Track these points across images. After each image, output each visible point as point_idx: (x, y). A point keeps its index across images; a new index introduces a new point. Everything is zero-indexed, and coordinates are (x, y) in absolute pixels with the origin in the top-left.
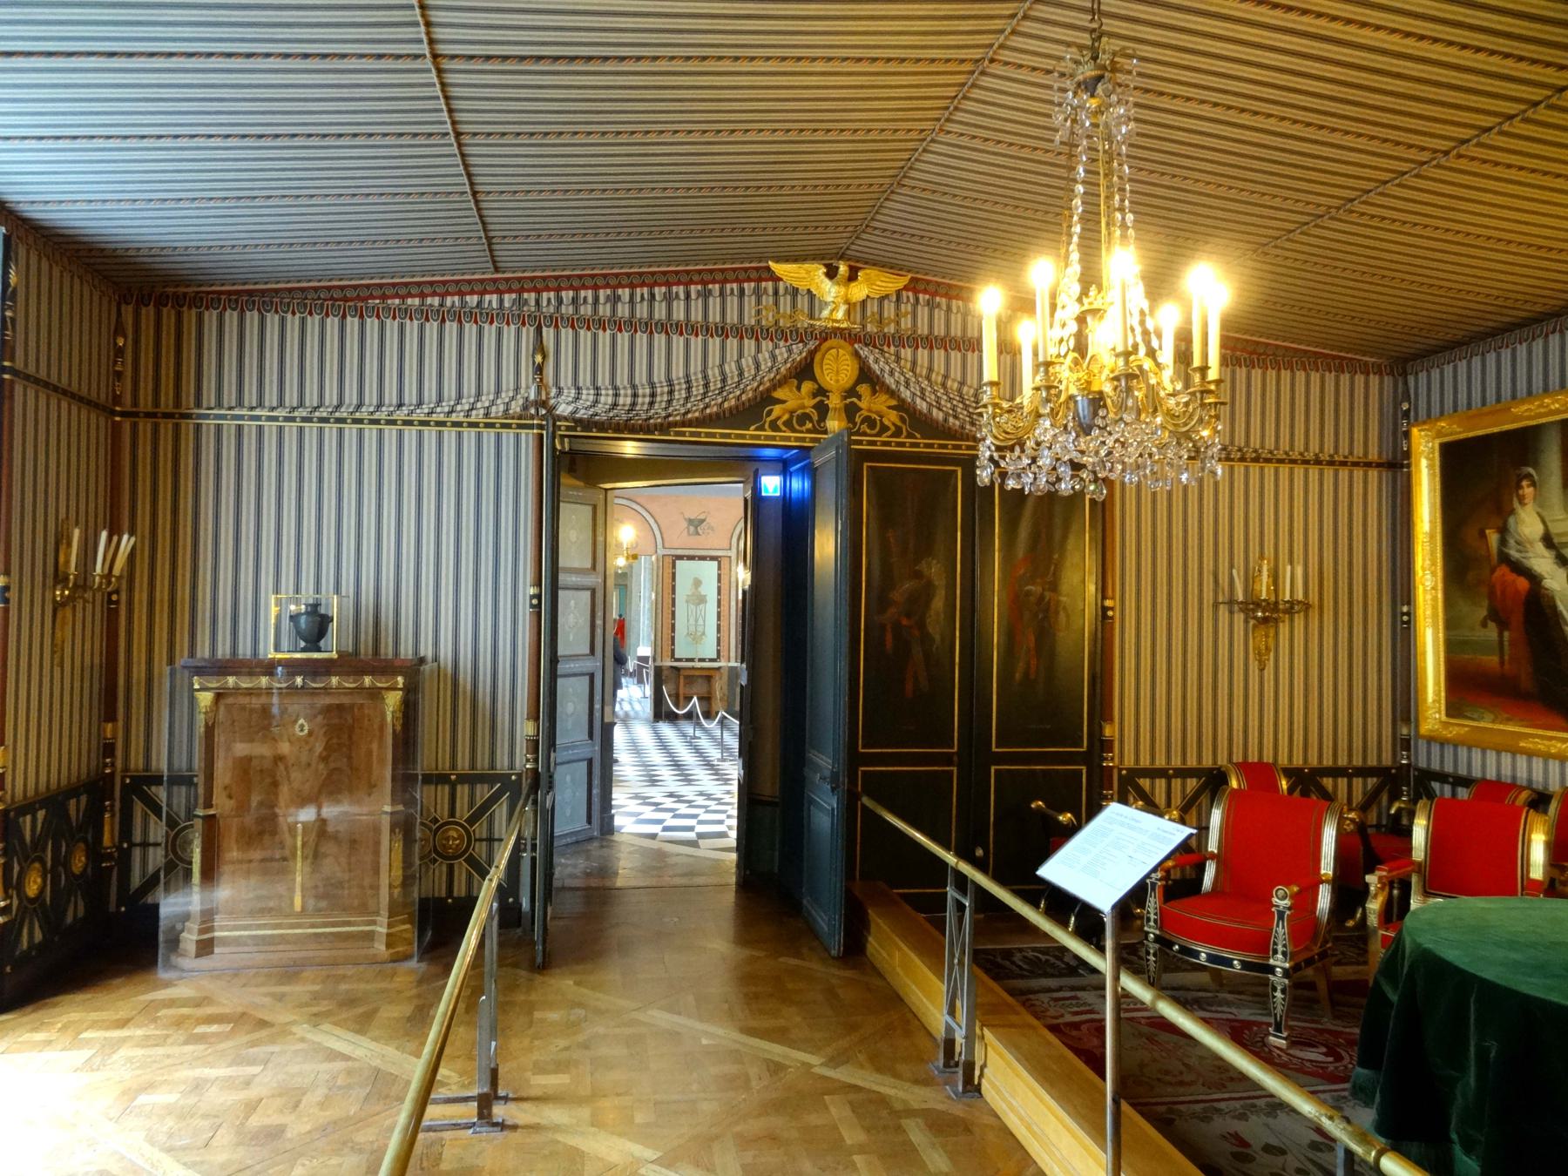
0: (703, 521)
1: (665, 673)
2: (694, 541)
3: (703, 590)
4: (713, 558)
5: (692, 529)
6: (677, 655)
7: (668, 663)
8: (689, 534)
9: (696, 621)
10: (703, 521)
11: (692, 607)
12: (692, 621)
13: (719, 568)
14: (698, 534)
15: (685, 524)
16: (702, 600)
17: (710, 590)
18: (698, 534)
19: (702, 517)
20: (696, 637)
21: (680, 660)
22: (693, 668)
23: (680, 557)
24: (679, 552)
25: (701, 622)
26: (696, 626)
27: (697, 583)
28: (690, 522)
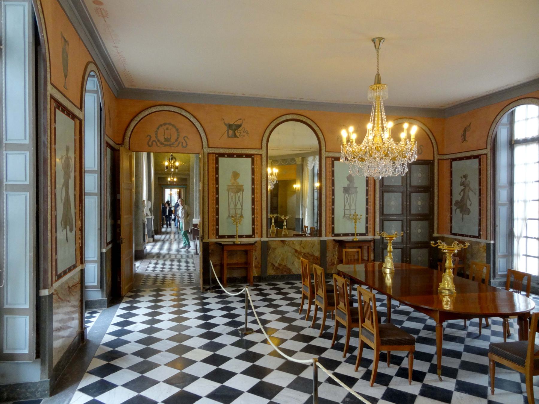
0: (239, 126)
1: (212, 247)
2: (233, 142)
3: (240, 181)
4: (248, 156)
5: (231, 132)
6: (221, 233)
7: (214, 240)
8: (229, 137)
9: (236, 205)
10: (239, 126)
11: (232, 194)
12: (232, 206)
13: (253, 163)
14: (235, 136)
15: (225, 128)
16: (240, 189)
17: (246, 180)
18: (235, 136)
19: (239, 123)
20: (236, 219)
21: (223, 237)
22: (235, 244)
23: (222, 155)
24: (221, 151)
25: (239, 206)
26: (236, 209)
27: (236, 175)
28: (230, 126)
